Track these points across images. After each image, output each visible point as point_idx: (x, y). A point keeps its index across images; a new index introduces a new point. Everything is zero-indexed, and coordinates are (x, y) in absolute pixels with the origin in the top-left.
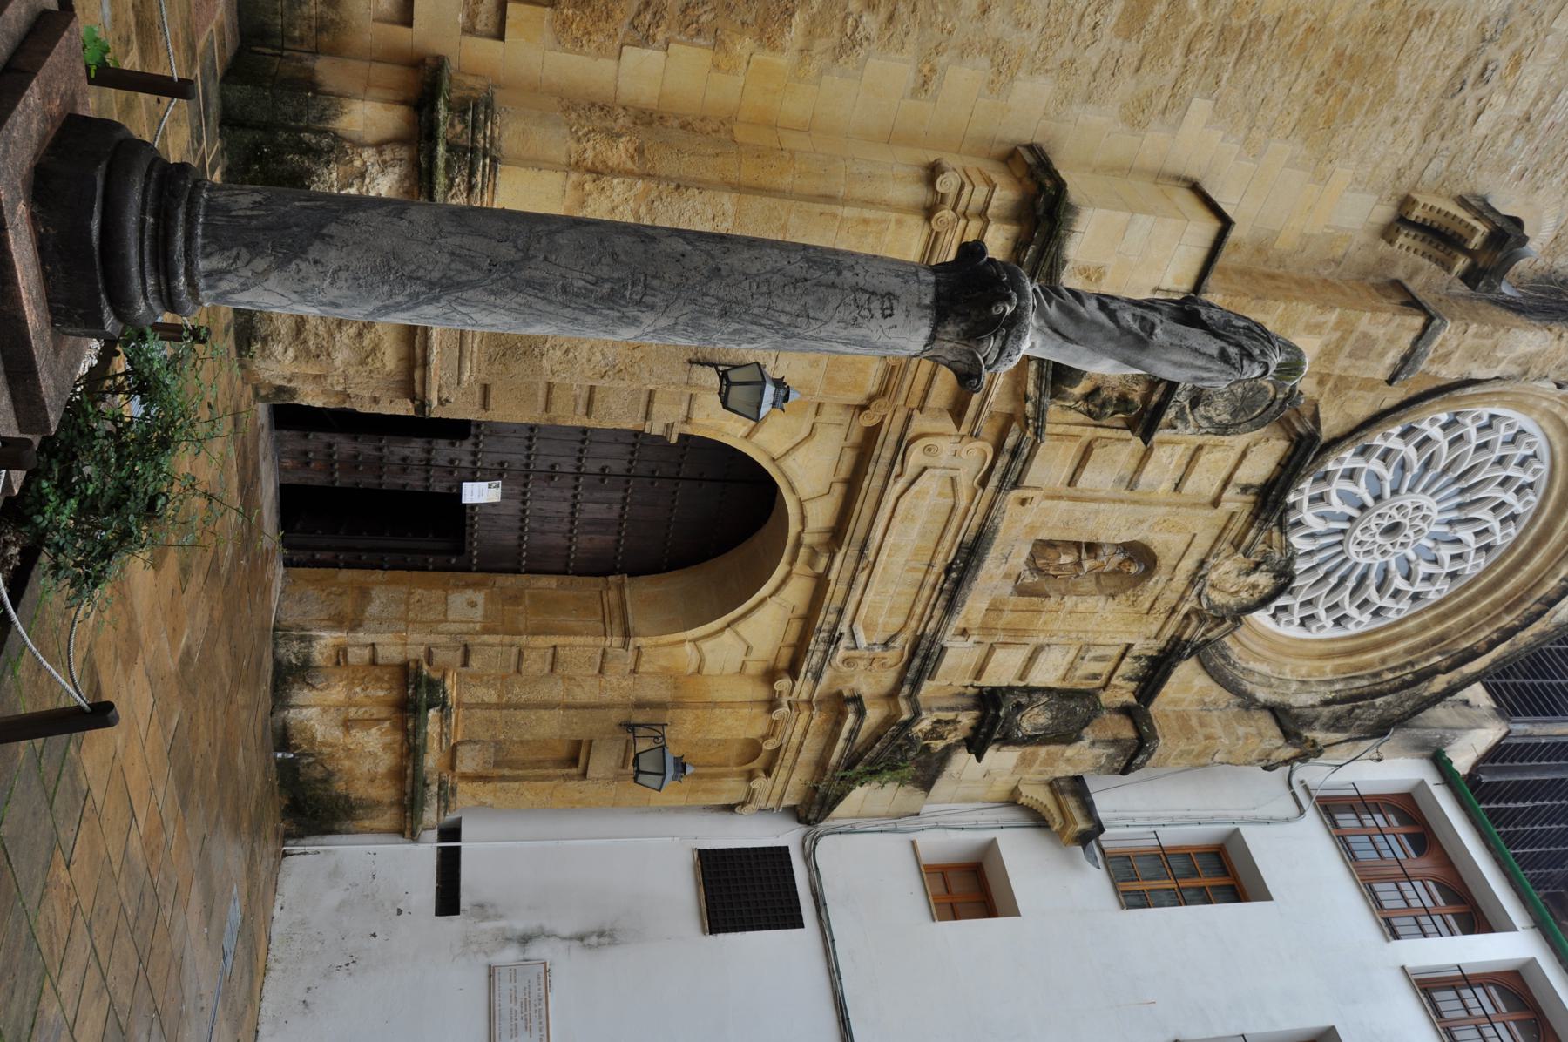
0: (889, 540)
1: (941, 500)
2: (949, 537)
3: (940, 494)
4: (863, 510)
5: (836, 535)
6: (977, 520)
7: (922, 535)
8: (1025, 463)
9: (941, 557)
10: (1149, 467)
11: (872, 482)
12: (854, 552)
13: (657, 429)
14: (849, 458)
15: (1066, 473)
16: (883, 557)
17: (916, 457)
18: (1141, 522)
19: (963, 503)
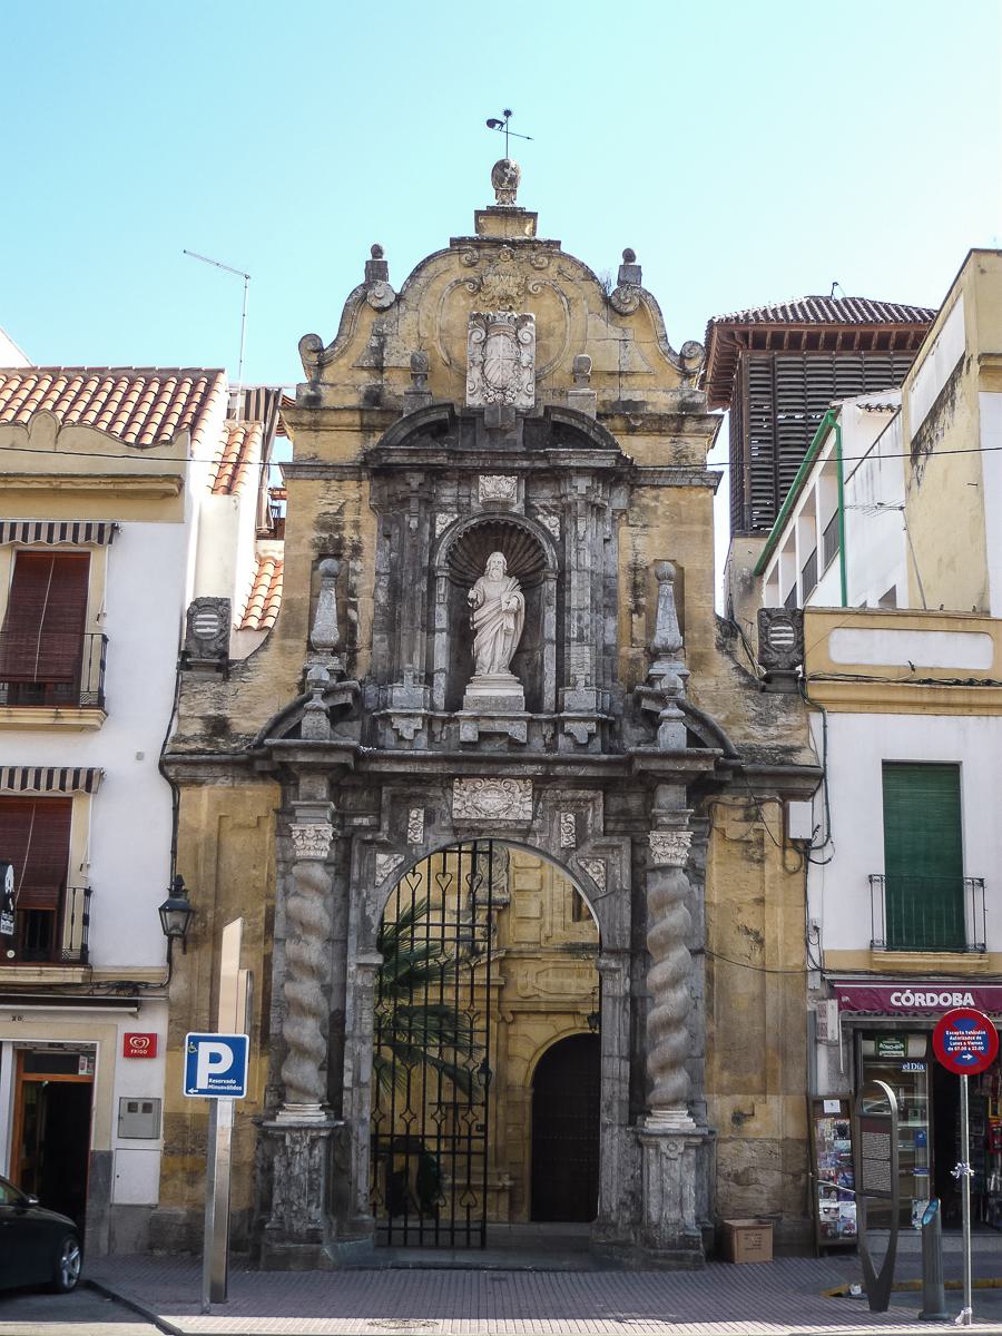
0: (573, 990)
1: (551, 975)
2: (568, 965)
3: (547, 975)
4: (558, 1007)
5: (575, 1013)
6: (559, 956)
7: (570, 976)
8: (529, 943)
9: (581, 965)
10: (527, 888)
11: (543, 1008)
12: (581, 1006)
13: (528, 1098)
14: (534, 1017)
15: (534, 922)
16: (583, 992)
17: (529, 992)
18: (558, 876)
19: (550, 965)
